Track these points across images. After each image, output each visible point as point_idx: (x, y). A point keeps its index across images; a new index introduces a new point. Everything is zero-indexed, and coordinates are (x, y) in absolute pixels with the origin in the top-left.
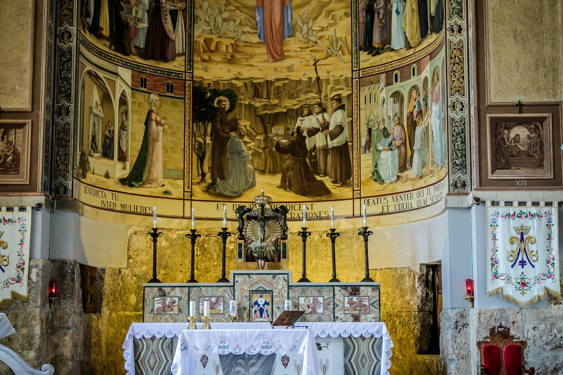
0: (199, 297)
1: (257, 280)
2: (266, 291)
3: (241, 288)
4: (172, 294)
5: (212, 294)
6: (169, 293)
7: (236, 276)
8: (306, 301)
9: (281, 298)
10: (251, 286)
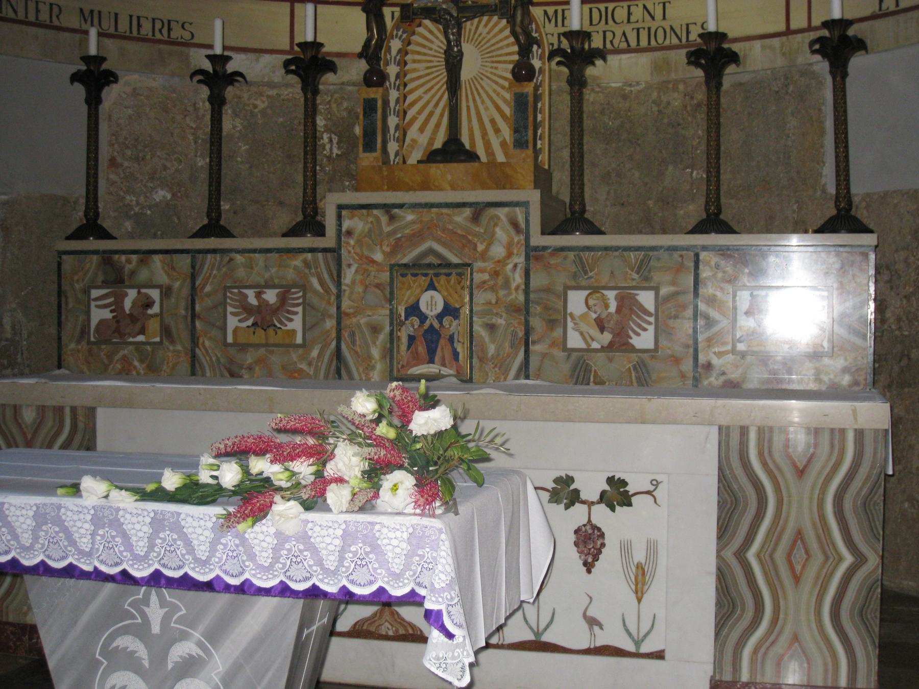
0: (226, 289)
1: (417, 227)
2: (449, 265)
3: (361, 256)
4: (143, 275)
5: (267, 276)
6: (133, 273)
7: (344, 213)
8: (591, 302)
9: (502, 293)
10: (397, 247)
